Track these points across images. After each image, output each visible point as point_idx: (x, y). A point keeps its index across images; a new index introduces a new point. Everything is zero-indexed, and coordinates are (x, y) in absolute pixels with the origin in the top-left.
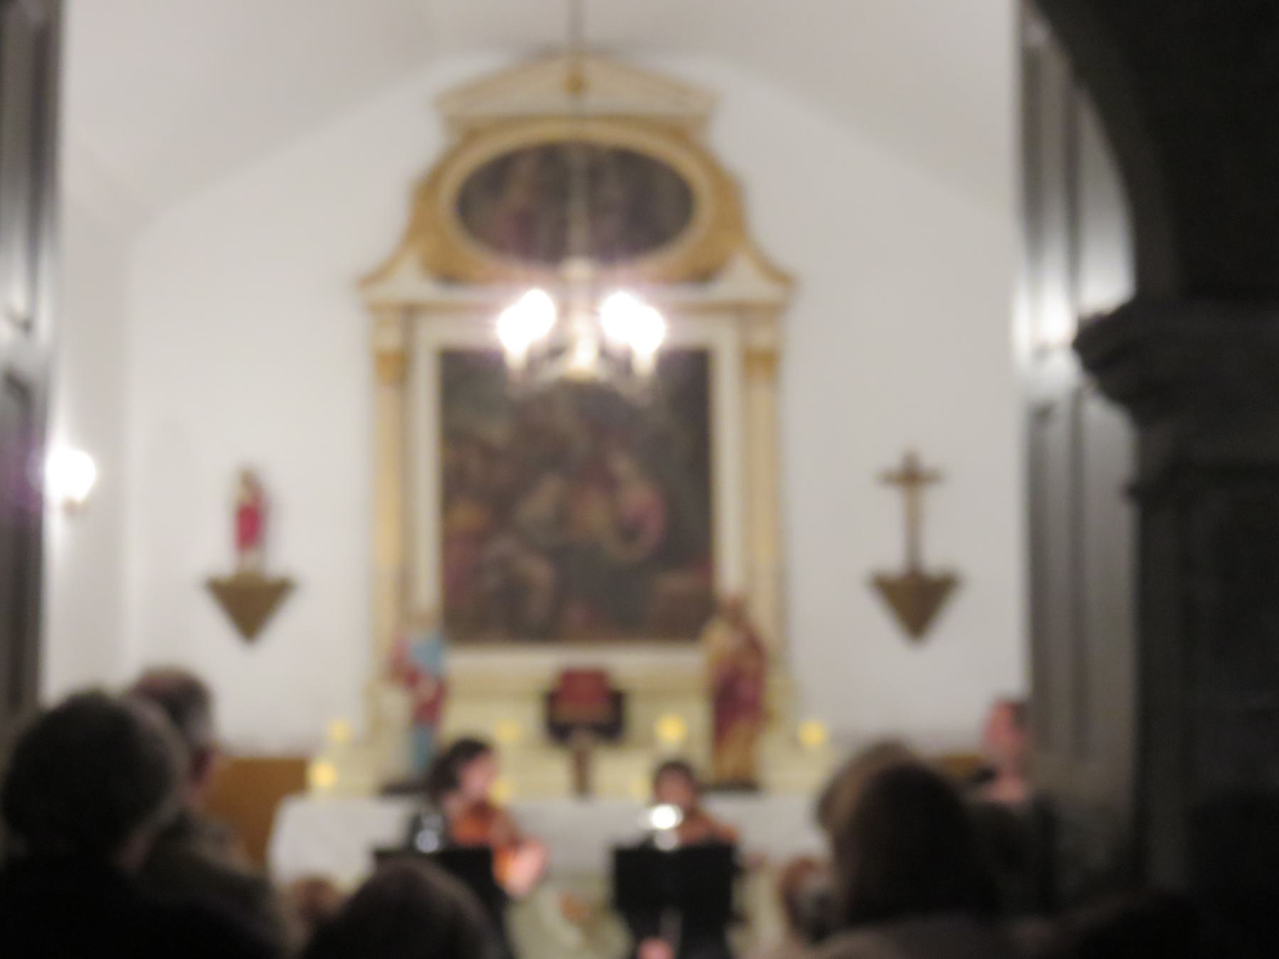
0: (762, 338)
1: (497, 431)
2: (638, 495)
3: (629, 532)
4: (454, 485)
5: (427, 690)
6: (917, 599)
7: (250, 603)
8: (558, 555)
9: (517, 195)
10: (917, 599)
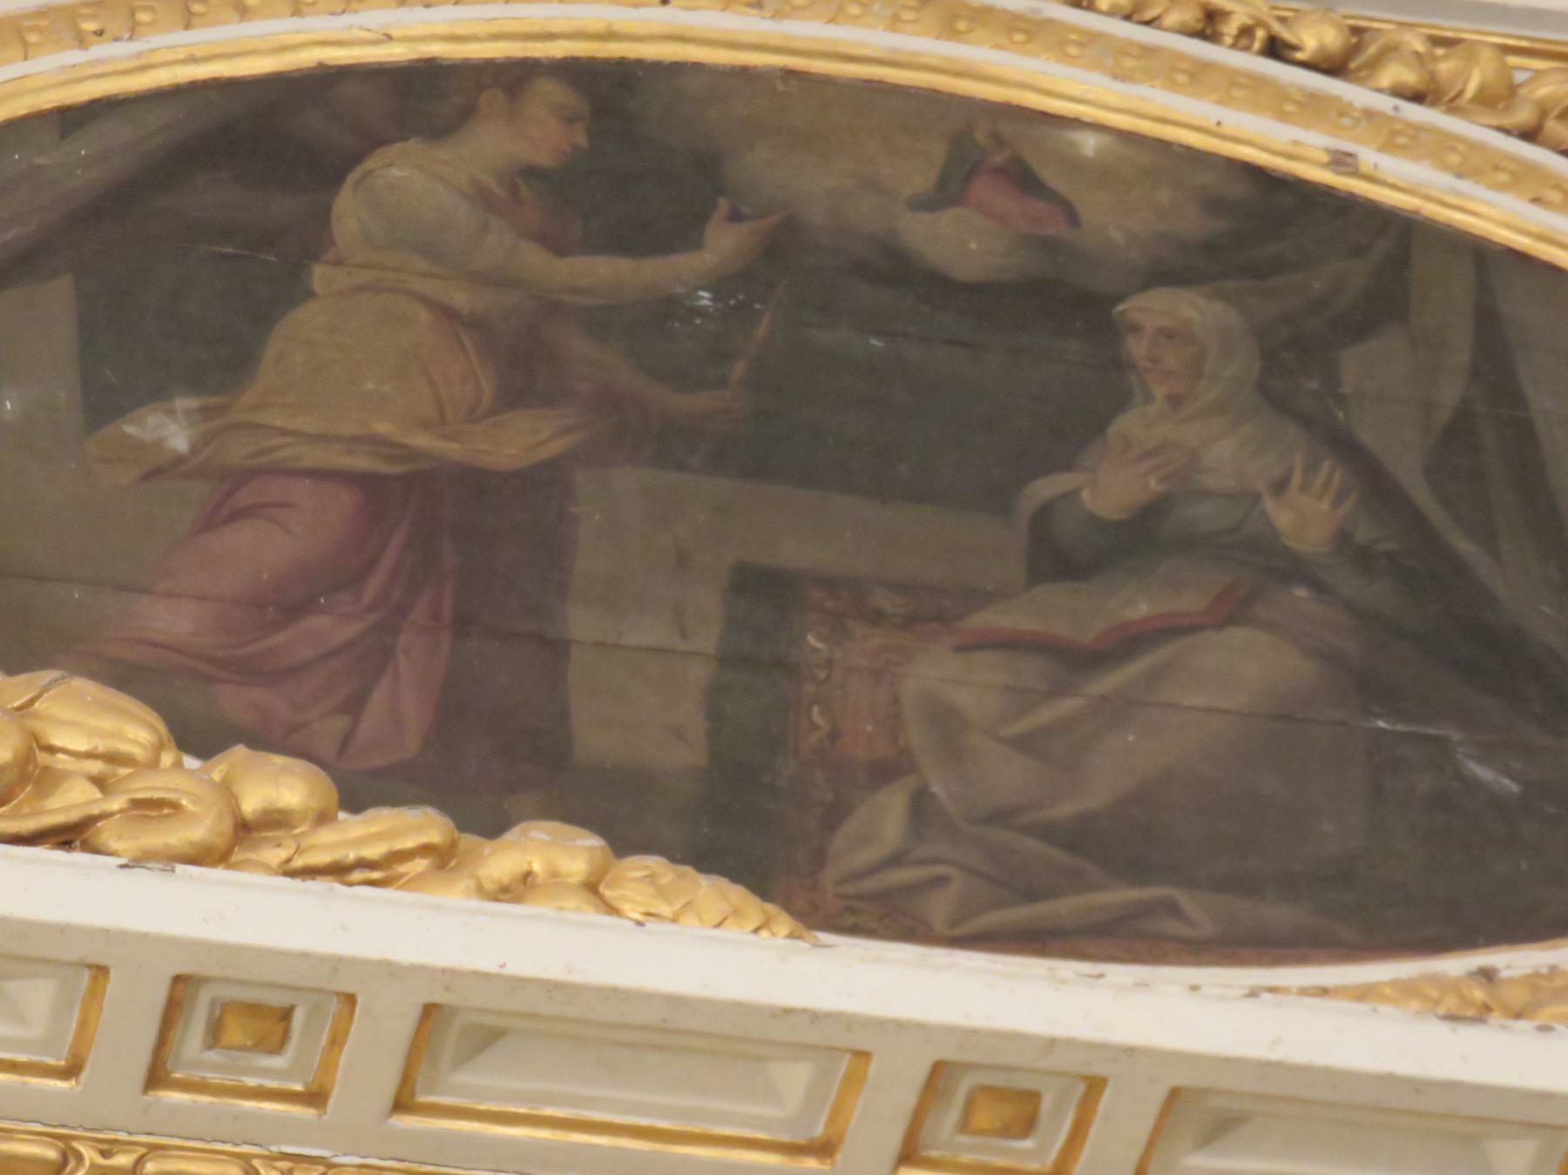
9: (360, 369)
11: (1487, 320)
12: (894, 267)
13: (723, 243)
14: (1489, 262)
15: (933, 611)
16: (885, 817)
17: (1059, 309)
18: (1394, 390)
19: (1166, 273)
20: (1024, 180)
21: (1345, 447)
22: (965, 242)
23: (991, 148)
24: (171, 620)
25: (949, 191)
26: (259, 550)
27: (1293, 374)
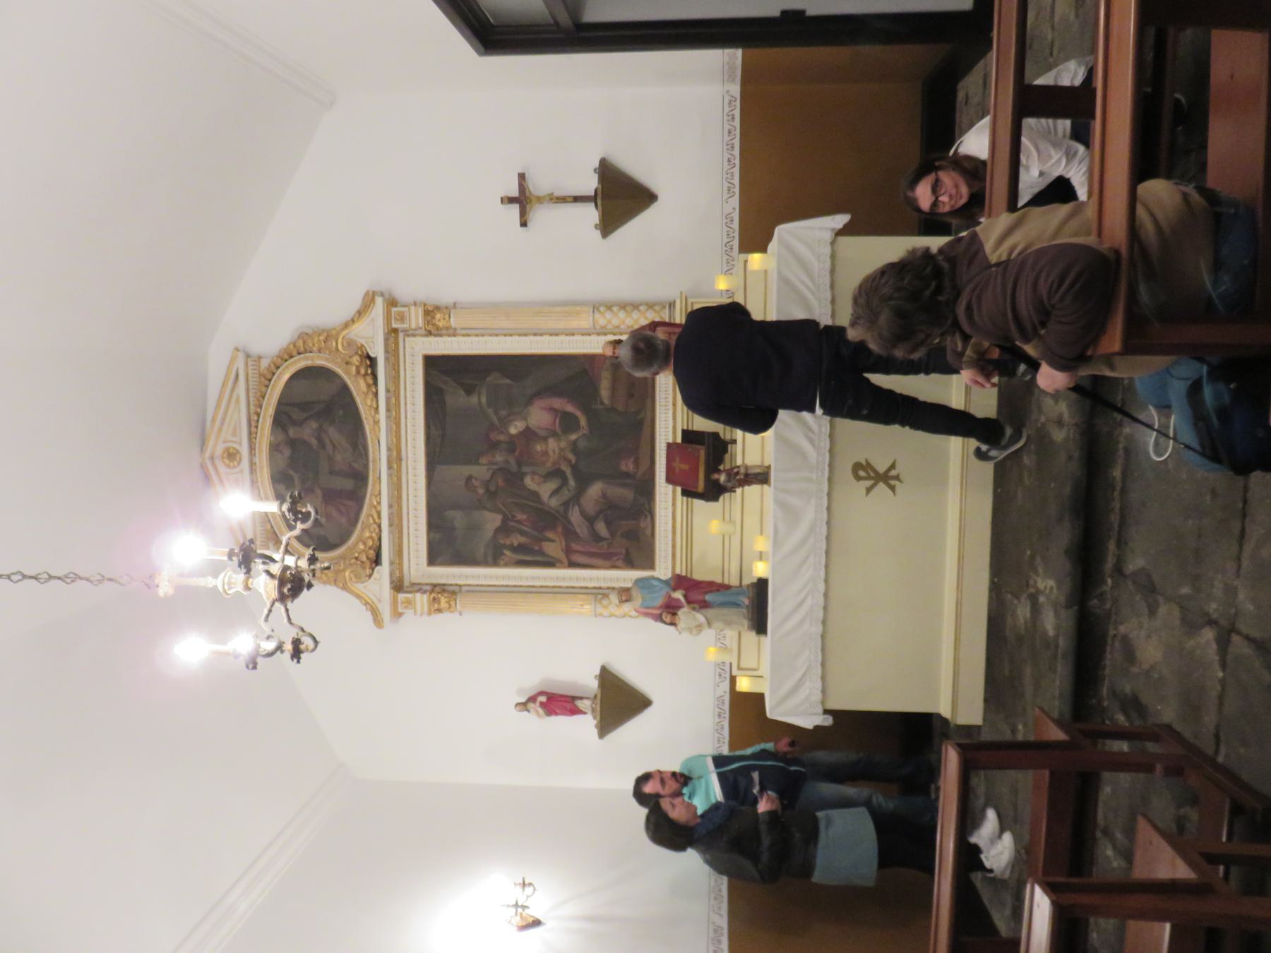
0: (416, 319)
1: (492, 521)
2: (538, 416)
3: (568, 422)
4: (532, 556)
5: (678, 595)
6: (620, 197)
7: (619, 702)
8: (583, 482)
10: (620, 197)
11: (286, 404)
12: (292, 458)
13: (291, 472)
14: (280, 403)
15: (330, 458)
16: (355, 465)
17: (293, 443)
18: (296, 414)
19: (287, 433)
20: (278, 445)
21: (306, 419)
22: (287, 452)
23: (274, 448)
24: (343, 520)
25: (281, 452)
26: (335, 513)
27: (298, 424)
